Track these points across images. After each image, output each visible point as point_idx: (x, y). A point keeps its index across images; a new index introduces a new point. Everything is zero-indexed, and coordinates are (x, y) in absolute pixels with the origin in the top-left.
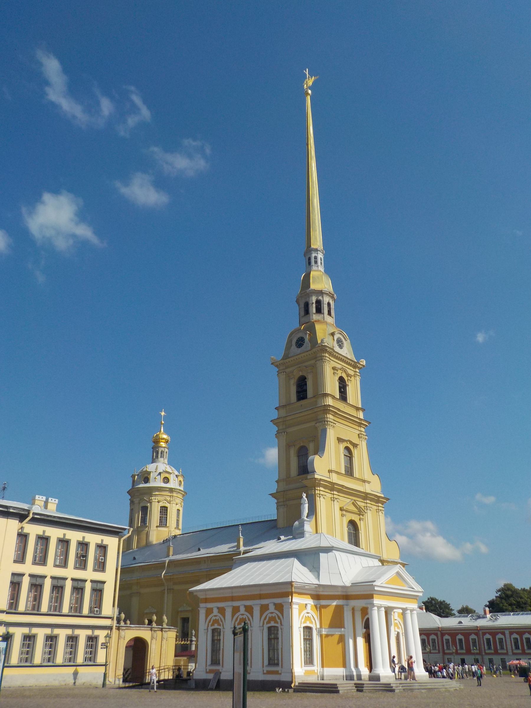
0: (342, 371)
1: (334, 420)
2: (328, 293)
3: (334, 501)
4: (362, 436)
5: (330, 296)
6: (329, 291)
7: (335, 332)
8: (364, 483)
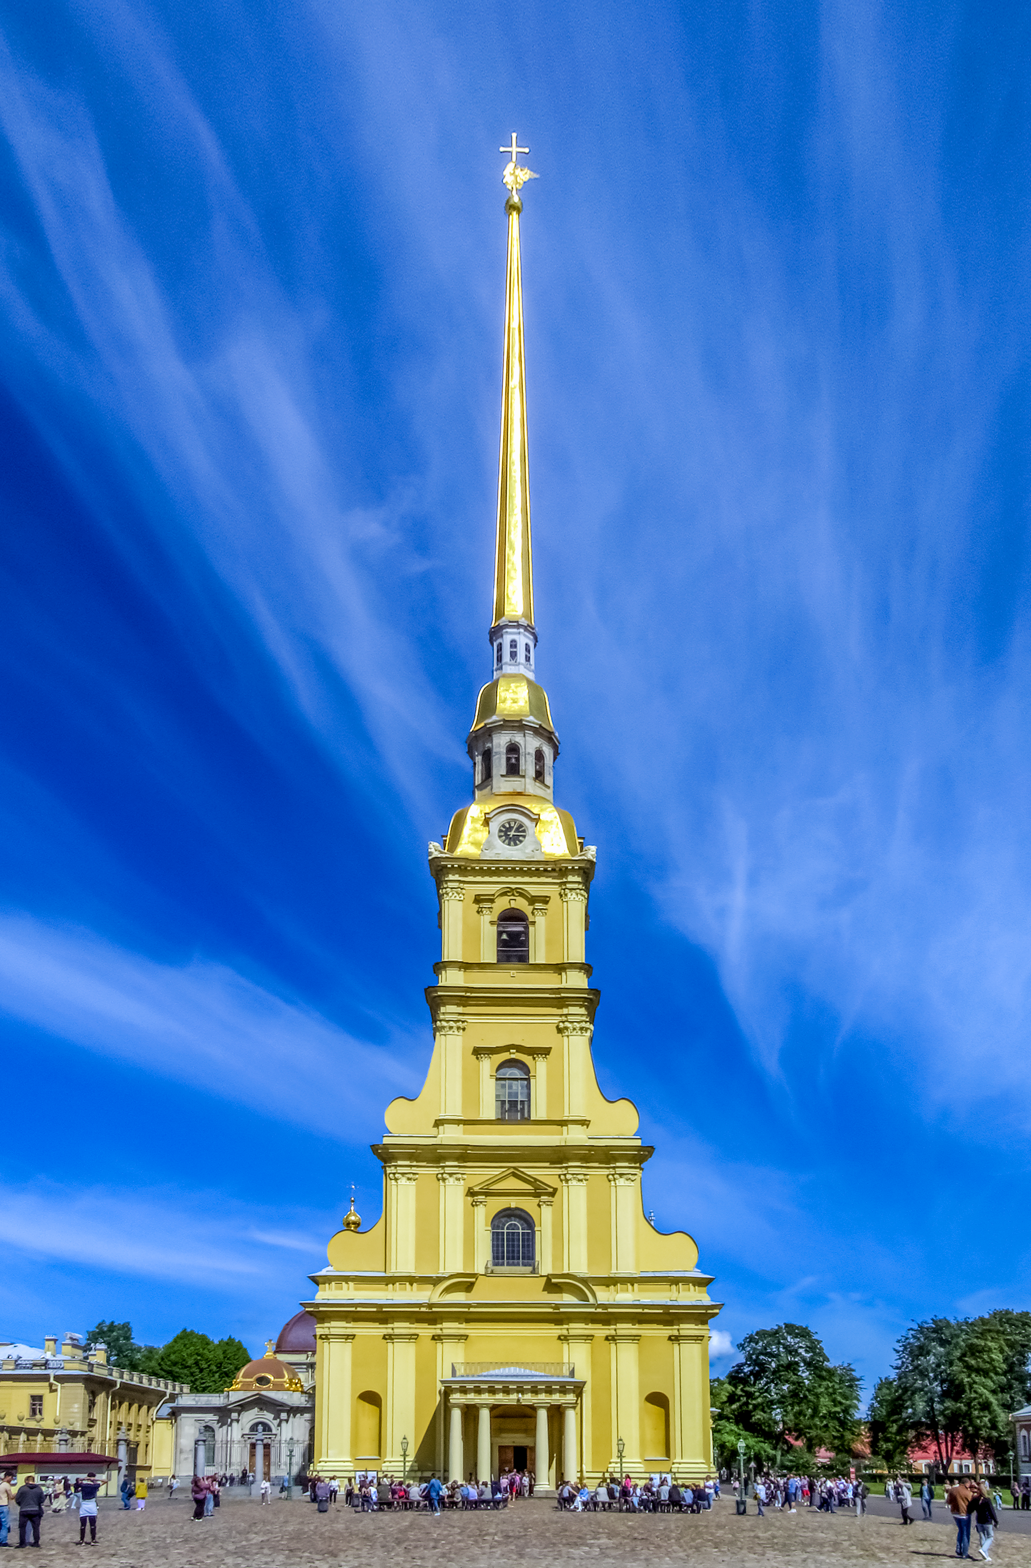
0: (513, 895)
1: (460, 1014)
2: (502, 723)
3: (444, 1180)
4: (567, 1024)
5: (513, 728)
6: (501, 718)
7: (488, 813)
8: (565, 1128)
